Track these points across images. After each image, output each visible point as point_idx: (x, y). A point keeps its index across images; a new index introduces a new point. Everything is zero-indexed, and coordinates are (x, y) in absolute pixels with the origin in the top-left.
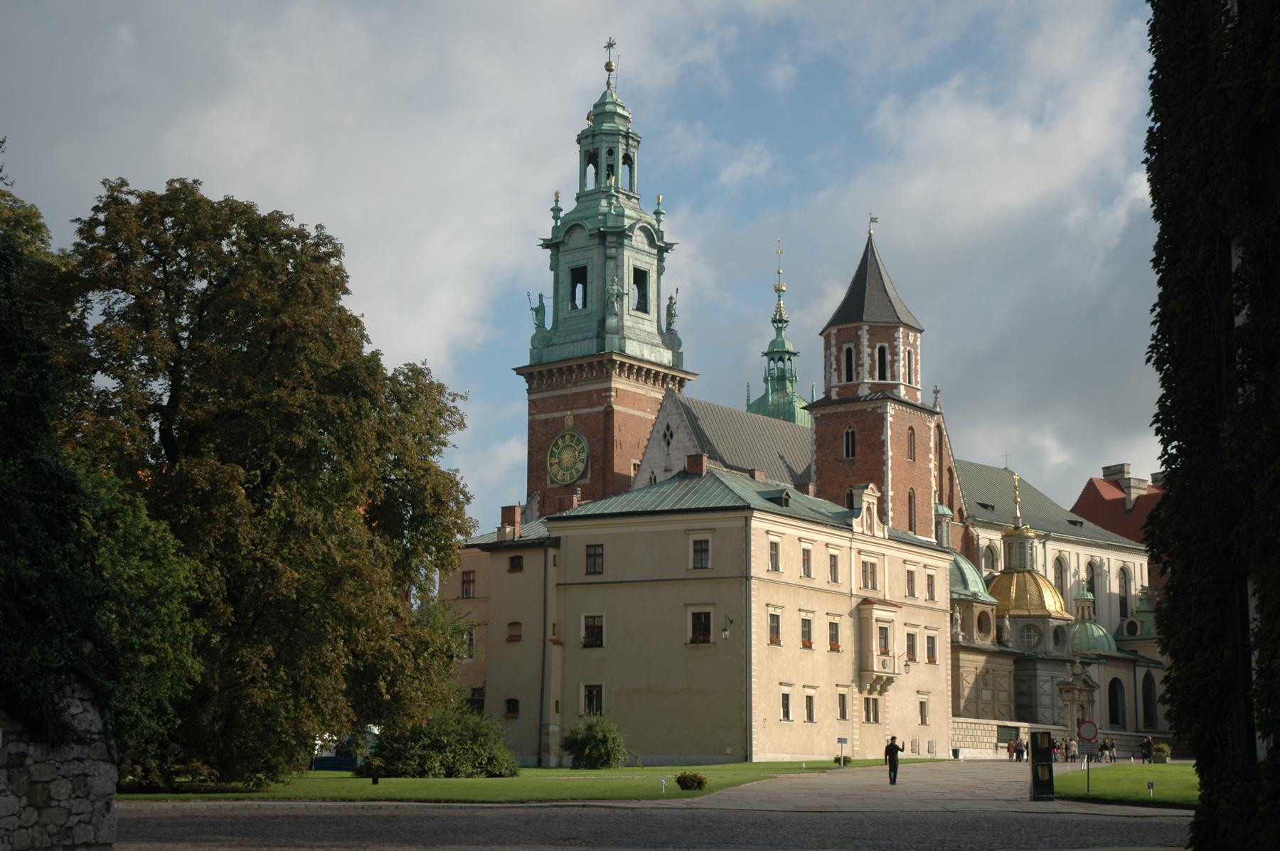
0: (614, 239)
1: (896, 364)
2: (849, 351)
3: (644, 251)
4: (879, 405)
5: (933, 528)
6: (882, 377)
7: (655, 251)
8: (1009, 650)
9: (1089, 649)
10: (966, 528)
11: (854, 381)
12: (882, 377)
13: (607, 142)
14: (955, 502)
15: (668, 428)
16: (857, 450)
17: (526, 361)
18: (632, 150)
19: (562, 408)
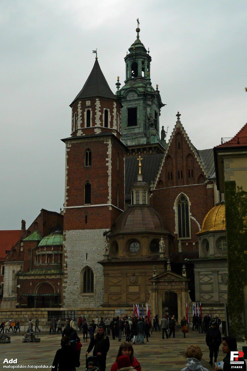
1: (78, 120)
5: (109, 197)
10: (206, 184)
18: (137, 60)
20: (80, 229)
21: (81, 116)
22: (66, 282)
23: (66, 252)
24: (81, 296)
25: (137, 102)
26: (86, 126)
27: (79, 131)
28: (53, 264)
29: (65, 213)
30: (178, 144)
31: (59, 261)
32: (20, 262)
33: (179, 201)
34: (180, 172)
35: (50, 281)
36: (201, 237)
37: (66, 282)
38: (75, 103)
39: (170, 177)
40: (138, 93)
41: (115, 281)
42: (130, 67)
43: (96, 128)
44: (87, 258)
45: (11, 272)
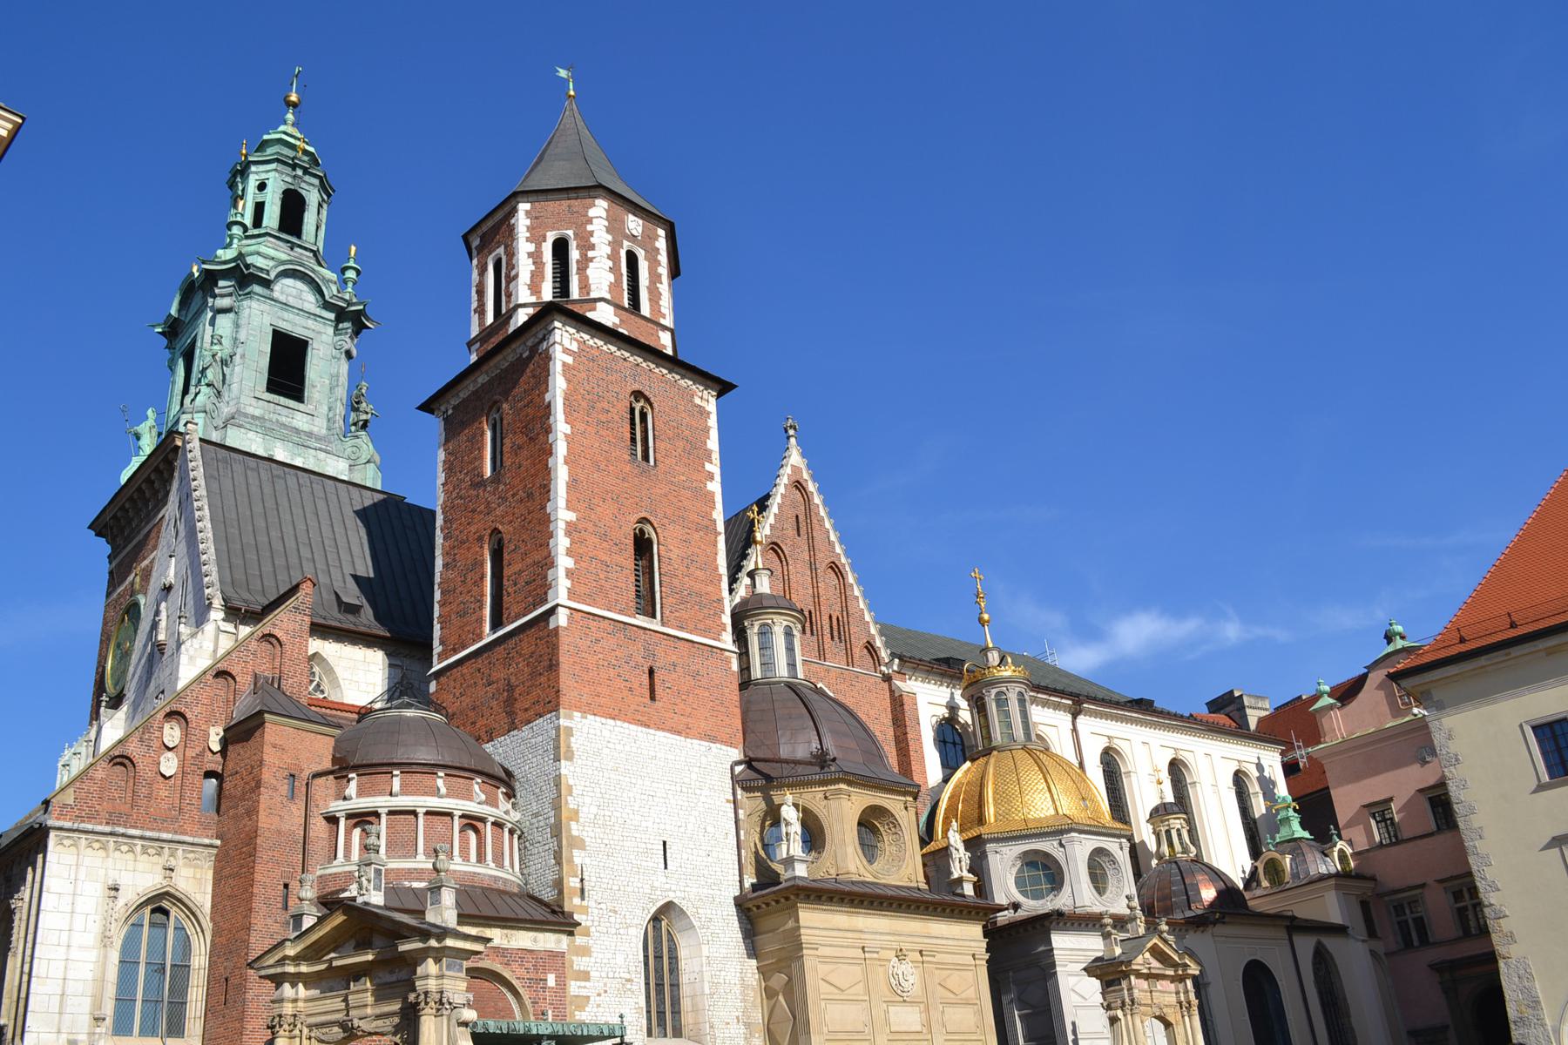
1: (591, 264)
3: (302, 310)
4: (540, 336)
5: (727, 619)
7: (332, 316)
10: (887, 679)
13: (256, 173)
18: (303, 185)
20: (630, 723)
21: (609, 258)
22: (585, 976)
23: (575, 815)
25: (310, 322)
26: (626, 303)
29: (565, 628)
30: (794, 519)
31: (507, 862)
32: (165, 836)
37: (585, 976)
40: (327, 298)
43: (665, 328)
44: (666, 868)
45: (93, 893)
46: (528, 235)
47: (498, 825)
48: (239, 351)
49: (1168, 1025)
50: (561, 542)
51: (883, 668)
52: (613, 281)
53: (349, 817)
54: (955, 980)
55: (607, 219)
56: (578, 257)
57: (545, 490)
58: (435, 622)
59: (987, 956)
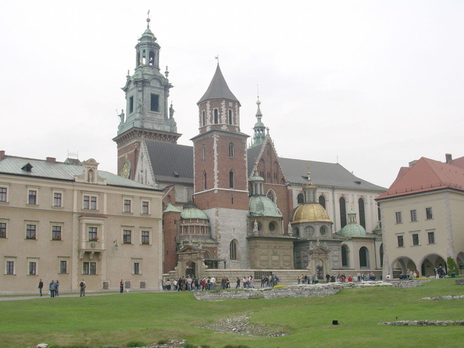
0: (141, 83)
1: (222, 116)
2: (204, 112)
4: (212, 134)
5: (247, 186)
6: (216, 122)
7: (163, 87)
8: (289, 237)
9: (351, 235)
10: (287, 186)
11: (205, 125)
12: (216, 122)
13: (143, 47)
14: (279, 176)
15: (142, 154)
16: (207, 155)
17: (116, 135)
18: (154, 49)
19: (125, 152)
21: (225, 114)
22: (220, 251)
23: (219, 225)
24: (232, 262)
27: (223, 126)
28: (206, 235)
33: (268, 195)
34: (269, 173)
35: (208, 249)
36: (303, 224)
37: (220, 251)
38: (216, 100)
39: (262, 175)
41: (263, 251)
42: (148, 54)
46: (209, 109)
47: (207, 227)
48: (144, 101)
49: (323, 261)
50: (216, 177)
51: (286, 184)
52: (226, 119)
53: (184, 226)
54: (286, 252)
55: (225, 105)
56: (219, 114)
57: (213, 166)
58: (194, 185)
59: (293, 247)
